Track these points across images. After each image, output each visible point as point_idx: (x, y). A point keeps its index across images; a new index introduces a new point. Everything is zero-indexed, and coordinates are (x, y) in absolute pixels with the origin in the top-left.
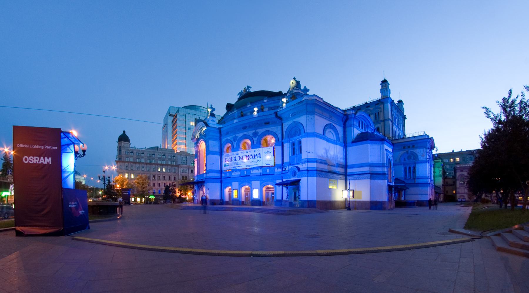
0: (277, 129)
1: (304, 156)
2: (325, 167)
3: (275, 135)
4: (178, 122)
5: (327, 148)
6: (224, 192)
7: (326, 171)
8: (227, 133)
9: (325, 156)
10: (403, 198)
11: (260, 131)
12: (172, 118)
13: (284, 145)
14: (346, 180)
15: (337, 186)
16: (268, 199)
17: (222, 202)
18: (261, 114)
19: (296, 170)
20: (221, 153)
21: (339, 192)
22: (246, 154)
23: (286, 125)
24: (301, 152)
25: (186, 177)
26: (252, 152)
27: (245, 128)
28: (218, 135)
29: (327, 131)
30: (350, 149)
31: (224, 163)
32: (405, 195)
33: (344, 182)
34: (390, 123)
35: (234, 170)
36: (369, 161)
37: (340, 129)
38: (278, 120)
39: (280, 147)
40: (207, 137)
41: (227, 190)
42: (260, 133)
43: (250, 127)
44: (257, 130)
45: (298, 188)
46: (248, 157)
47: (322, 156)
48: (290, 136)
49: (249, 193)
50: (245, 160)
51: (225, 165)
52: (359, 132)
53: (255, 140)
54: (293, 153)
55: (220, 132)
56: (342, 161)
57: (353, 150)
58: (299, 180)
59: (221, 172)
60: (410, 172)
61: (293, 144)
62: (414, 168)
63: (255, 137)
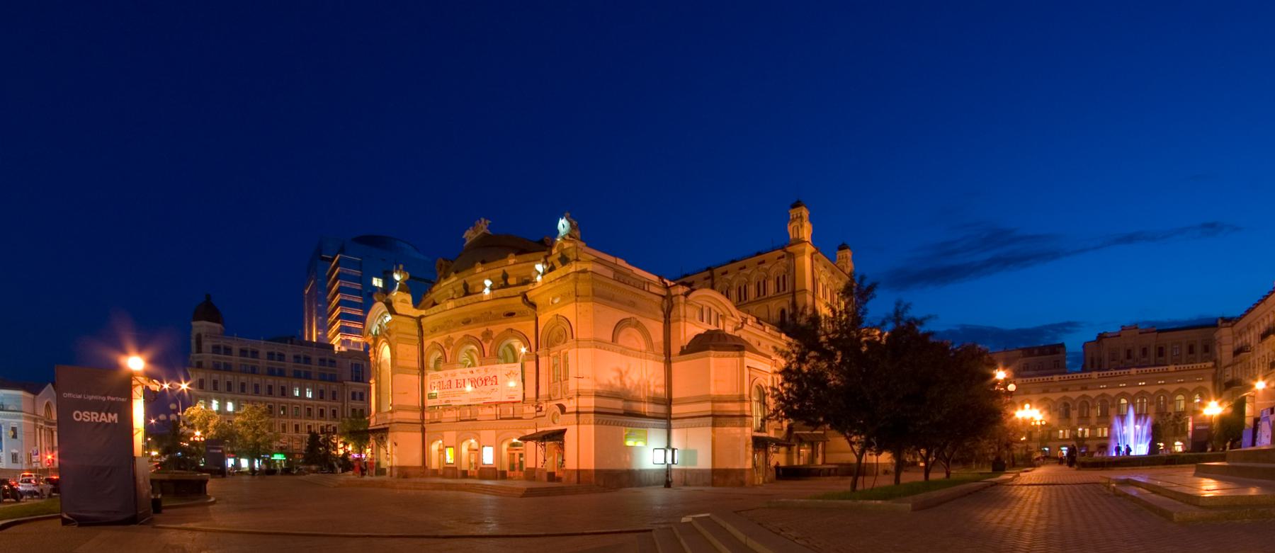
0: (527, 327)
2: (619, 405)
3: (526, 342)
5: (624, 369)
6: (430, 451)
7: (620, 412)
8: (434, 331)
9: (618, 384)
10: (819, 461)
11: (498, 328)
15: (646, 441)
16: (512, 468)
18: (499, 293)
19: (558, 411)
20: (422, 370)
21: (649, 452)
22: (471, 376)
23: (545, 318)
24: (566, 379)
26: (480, 372)
27: (467, 322)
28: (416, 332)
29: (622, 334)
30: (679, 367)
31: (428, 391)
32: (824, 453)
33: (664, 432)
35: (448, 407)
36: (713, 391)
37: (656, 328)
38: (530, 310)
39: (534, 363)
40: (393, 337)
41: (435, 447)
42: (495, 335)
43: (477, 320)
44: (490, 328)
45: (562, 447)
48: (550, 345)
49: (478, 452)
50: (469, 388)
51: (431, 397)
52: (702, 331)
53: (487, 347)
55: (420, 326)
56: (661, 391)
57: (681, 367)
58: (565, 430)
59: (423, 409)
63: (487, 342)
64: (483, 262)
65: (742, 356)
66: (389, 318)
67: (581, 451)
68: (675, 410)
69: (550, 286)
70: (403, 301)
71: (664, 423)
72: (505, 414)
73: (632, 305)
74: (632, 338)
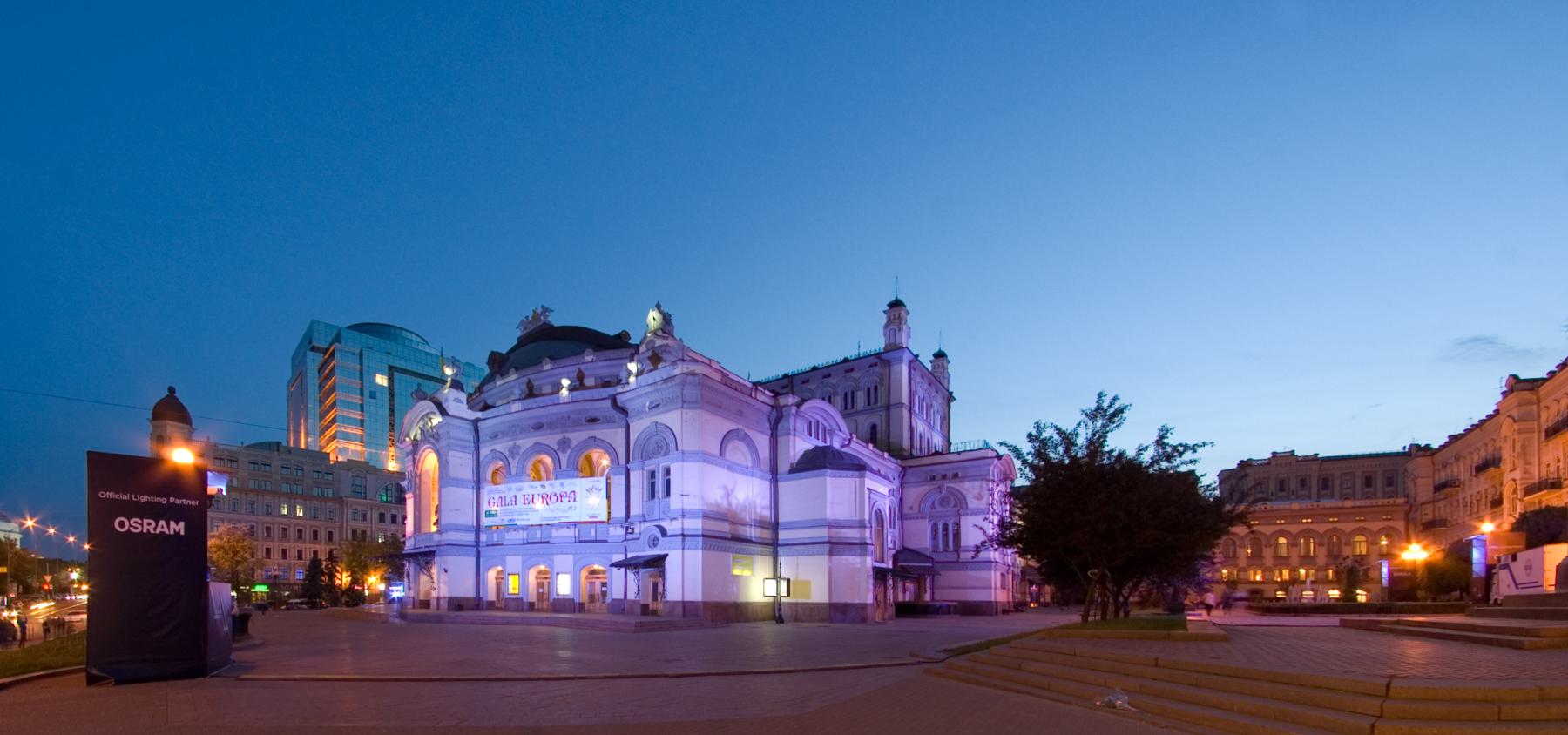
0: (616, 436)
1: (675, 502)
2: (725, 528)
3: (610, 449)
4: (337, 371)
5: (730, 486)
6: (486, 579)
7: (726, 536)
8: (495, 436)
9: (725, 503)
10: (927, 597)
11: (577, 437)
12: (320, 358)
13: (632, 474)
14: (775, 556)
15: (752, 569)
16: (592, 598)
17: (477, 604)
18: (579, 394)
19: (659, 534)
20: (478, 484)
21: (758, 584)
22: (542, 491)
23: (638, 427)
24: (668, 494)
25: (364, 533)
26: (554, 486)
27: (538, 427)
28: (471, 437)
29: (729, 448)
30: (788, 487)
31: (485, 507)
32: (932, 588)
33: (769, 560)
34: (906, 413)
35: (511, 527)
36: (830, 514)
37: (762, 441)
38: (618, 416)
39: (623, 478)
40: (443, 442)
42: (574, 443)
44: (568, 435)
45: (662, 575)
46: (547, 498)
47: (718, 505)
48: (645, 457)
49: (546, 579)
50: (539, 505)
51: (489, 514)
52: (809, 446)
53: (564, 458)
54: (652, 495)
55: (477, 431)
56: (767, 513)
57: (788, 487)
58: (665, 556)
59: (478, 529)
60: (946, 536)
61: (653, 474)
62: (958, 524)
63: (564, 451)
64: (552, 358)
65: (862, 477)
66: (437, 420)
67: (685, 577)
68: (783, 535)
69: (648, 389)
70: (457, 400)
71: (770, 549)
72: (587, 536)
73: (740, 414)
74: (738, 453)
